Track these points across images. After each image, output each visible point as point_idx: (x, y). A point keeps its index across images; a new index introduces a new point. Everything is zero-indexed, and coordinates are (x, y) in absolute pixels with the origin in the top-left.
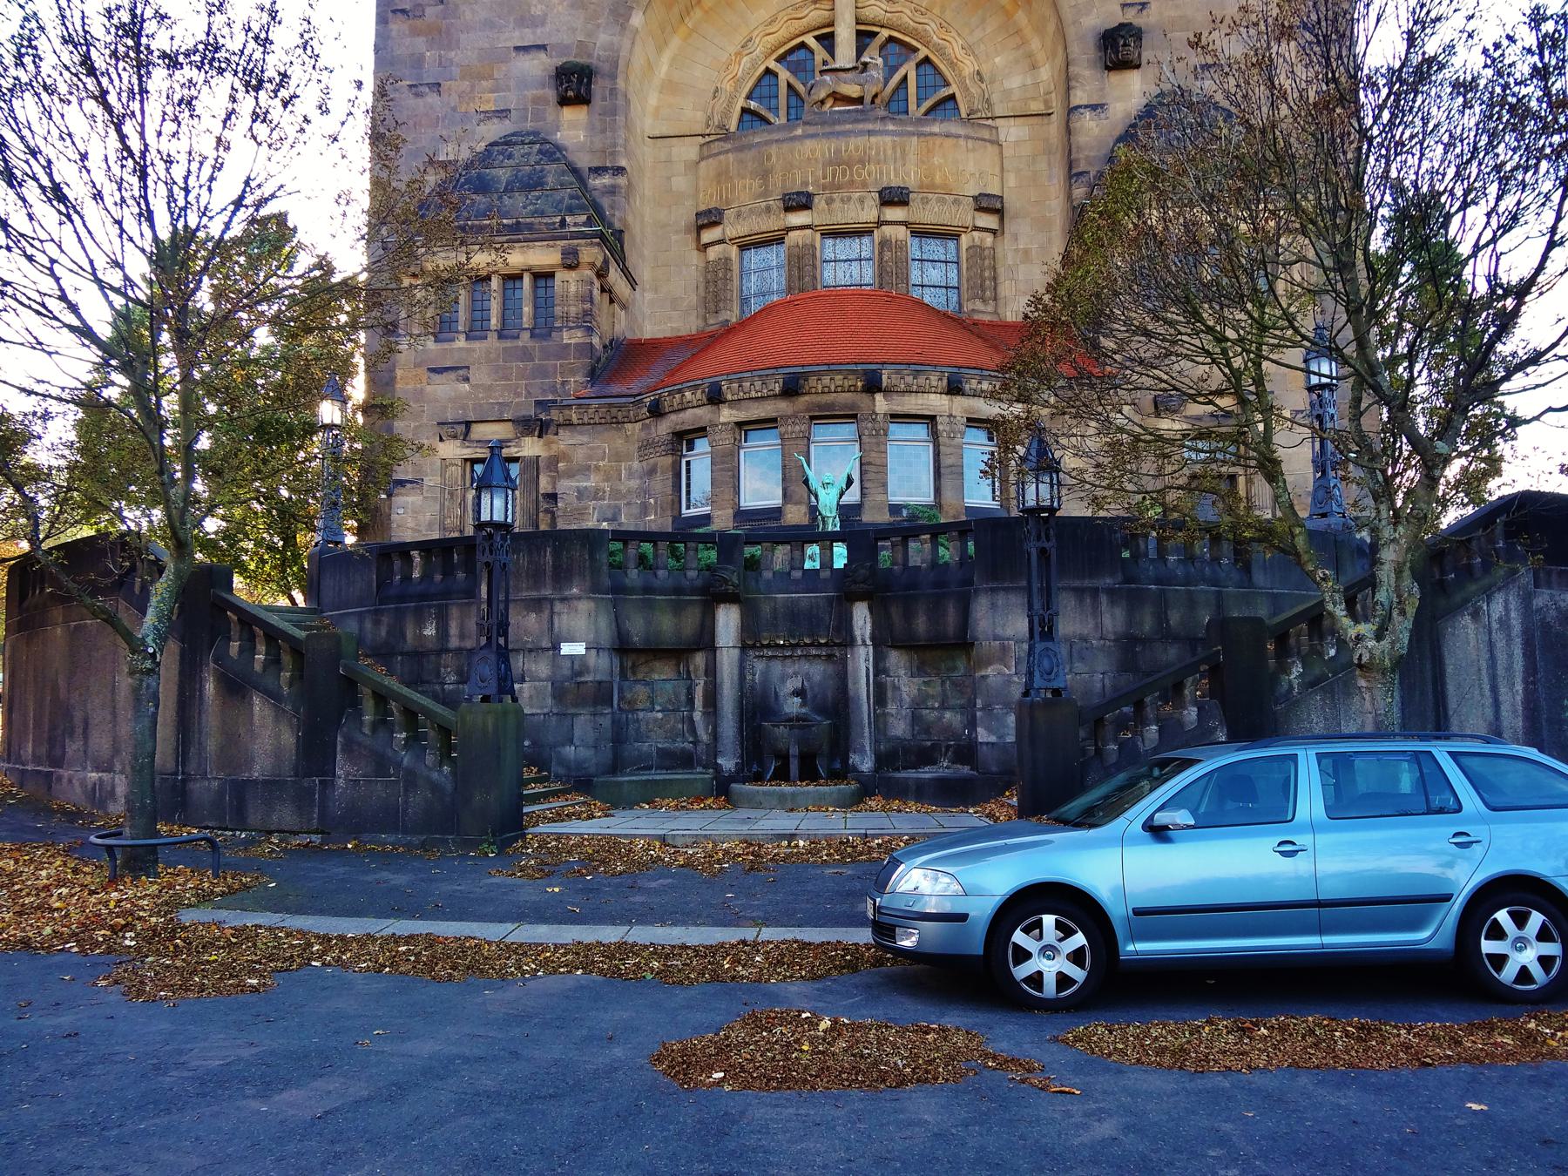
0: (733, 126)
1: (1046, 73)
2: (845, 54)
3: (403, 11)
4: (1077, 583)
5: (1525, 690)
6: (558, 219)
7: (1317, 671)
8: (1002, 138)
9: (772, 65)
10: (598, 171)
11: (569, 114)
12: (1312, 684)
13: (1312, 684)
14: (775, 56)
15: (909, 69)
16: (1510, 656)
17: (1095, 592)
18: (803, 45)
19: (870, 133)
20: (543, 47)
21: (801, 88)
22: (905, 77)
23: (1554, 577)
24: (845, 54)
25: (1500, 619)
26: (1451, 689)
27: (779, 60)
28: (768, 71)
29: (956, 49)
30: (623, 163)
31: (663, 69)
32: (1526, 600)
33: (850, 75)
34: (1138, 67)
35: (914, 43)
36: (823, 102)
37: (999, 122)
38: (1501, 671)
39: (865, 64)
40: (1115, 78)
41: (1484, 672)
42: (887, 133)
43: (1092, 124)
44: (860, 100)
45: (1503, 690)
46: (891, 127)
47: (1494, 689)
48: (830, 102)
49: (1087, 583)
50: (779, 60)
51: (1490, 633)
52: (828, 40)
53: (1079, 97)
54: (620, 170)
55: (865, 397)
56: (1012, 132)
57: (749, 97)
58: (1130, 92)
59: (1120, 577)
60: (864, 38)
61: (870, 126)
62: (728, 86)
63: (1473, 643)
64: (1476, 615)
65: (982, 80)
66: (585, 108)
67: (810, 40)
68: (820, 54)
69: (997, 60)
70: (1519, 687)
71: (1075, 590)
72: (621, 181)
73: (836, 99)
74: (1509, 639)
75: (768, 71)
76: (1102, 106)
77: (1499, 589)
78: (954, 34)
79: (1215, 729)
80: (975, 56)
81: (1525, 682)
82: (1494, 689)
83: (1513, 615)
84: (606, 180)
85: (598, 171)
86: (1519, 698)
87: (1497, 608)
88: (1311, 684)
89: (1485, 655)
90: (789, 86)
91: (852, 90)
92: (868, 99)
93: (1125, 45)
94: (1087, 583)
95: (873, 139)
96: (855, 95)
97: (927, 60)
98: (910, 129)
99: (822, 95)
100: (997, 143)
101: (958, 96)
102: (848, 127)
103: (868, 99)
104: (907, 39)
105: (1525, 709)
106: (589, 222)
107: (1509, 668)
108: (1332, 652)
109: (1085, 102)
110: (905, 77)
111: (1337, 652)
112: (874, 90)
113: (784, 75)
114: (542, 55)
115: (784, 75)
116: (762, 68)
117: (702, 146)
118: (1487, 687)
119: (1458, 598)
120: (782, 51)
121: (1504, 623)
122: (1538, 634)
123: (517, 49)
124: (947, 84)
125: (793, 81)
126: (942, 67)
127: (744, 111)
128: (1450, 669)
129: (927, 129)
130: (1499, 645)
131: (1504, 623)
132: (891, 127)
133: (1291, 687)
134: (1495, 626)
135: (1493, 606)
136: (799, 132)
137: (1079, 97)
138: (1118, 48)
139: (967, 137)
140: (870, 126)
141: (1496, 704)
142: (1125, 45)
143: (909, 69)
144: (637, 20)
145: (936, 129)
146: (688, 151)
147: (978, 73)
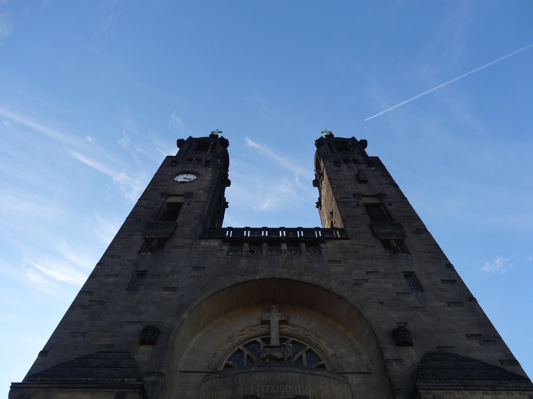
0: (221, 368)
1: (365, 357)
2: (275, 341)
3: (83, 306)
6: (120, 380)
8: (350, 382)
9: (241, 347)
10: (149, 374)
11: (143, 348)
14: (243, 344)
15: (303, 353)
18: (255, 342)
19: (288, 372)
20: (140, 322)
21: (253, 357)
22: (301, 357)
24: (275, 341)
27: (245, 346)
28: (239, 350)
29: (323, 345)
30: (164, 371)
31: (192, 344)
33: (277, 349)
34: (411, 345)
35: (304, 343)
36: (264, 359)
37: (348, 375)
39: (284, 346)
40: (402, 349)
42: (296, 372)
43: (398, 367)
44: (282, 359)
46: (298, 370)
48: (268, 360)
50: (245, 346)
52: (267, 340)
53: (388, 355)
54: (162, 374)
56: (354, 380)
57: (230, 359)
58: (412, 356)
60: (282, 340)
61: (288, 369)
62: (221, 354)
65: (336, 358)
66: (152, 346)
67: (259, 339)
68: (263, 345)
69: (342, 350)
72: (161, 379)
73: (271, 359)
75: (239, 350)
76: (400, 360)
78: (321, 339)
80: (333, 348)
84: (153, 378)
85: (149, 374)
90: (248, 357)
91: (279, 355)
92: (286, 359)
93: (404, 334)
95: (289, 374)
96: (280, 357)
97: (310, 351)
98: (307, 372)
99: (265, 355)
100: (348, 383)
101: (326, 364)
102: (277, 368)
103: (286, 359)
104: (301, 342)
106: (137, 381)
109: (391, 358)
110: (301, 357)
112: (289, 355)
113: (246, 352)
114: (139, 325)
115: (246, 352)
116: (237, 349)
117: (204, 377)
120: (246, 342)
123: (128, 322)
124: (320, 360)
125: (250, 354)
126: (317, 353)
127: (227, 366)
129: (315, 373)
132: (298, 370)
136: (253, 369)
137: (388, 355)
138: (401, 337)
139: (334, 379)
140: (288, 369)
142: (404, 334)
143: (303, 353)
144: (185, 316)
145: (319, 373)
146: (197, 378)
147: (335, 355)
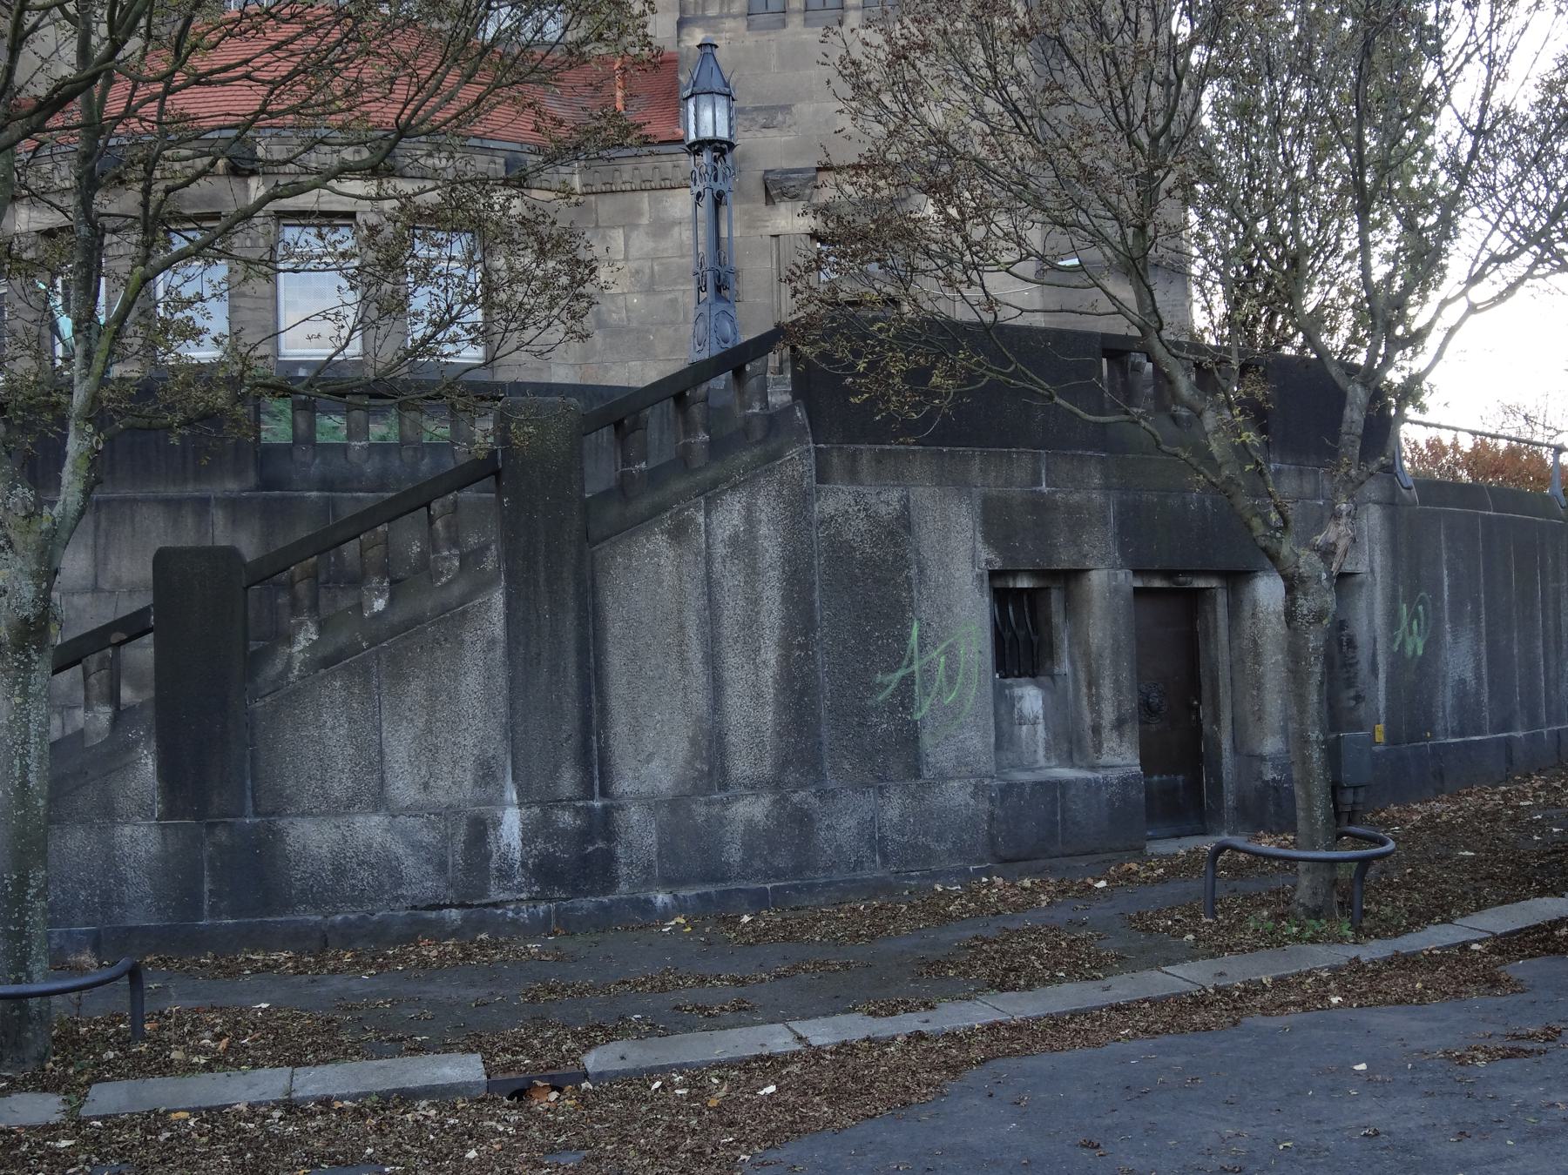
4: (172, 492)
5: (785, 658)
7: (343, 639)
12: (327, 662)
13: (327, 662)
16: (754, 601)
17: (203, 504)
23: (865, 462)
25: (734, 541)
26: (616, 660)
32: (798, 505)
38: (729, 626)
41: (692, 631)
45: (733, 660)
47: (713, 661)
49: (191, 490)
51: (709, 561)
55: (235, 183)
59: (252, 478)
63: (668, 580)
64: (679, 533)
70: (770, 655)
71: (167, 502)
74: (753, 573)
77: (734, 487)
79: (136, 742)
81: (786, 645)
82: (713, 661)
83: (763, 530)
86: (768, 675)
87: (729, 517)
88: (325, 662)
89: (695, 601)
94: (191, 490)
105: (780, 691)
107: (750, 624)
108: (380, 605)
111: (391, 602)
118: (695, 654)
119: (643, 505)
121: (744, 546)
122: (819, 562)
128: (615, 629)
130: (728, 583)
131: (744, 546)
133: (289, 667)
134: (720, 550)
135: (717, 517)
141: (717, 686)
